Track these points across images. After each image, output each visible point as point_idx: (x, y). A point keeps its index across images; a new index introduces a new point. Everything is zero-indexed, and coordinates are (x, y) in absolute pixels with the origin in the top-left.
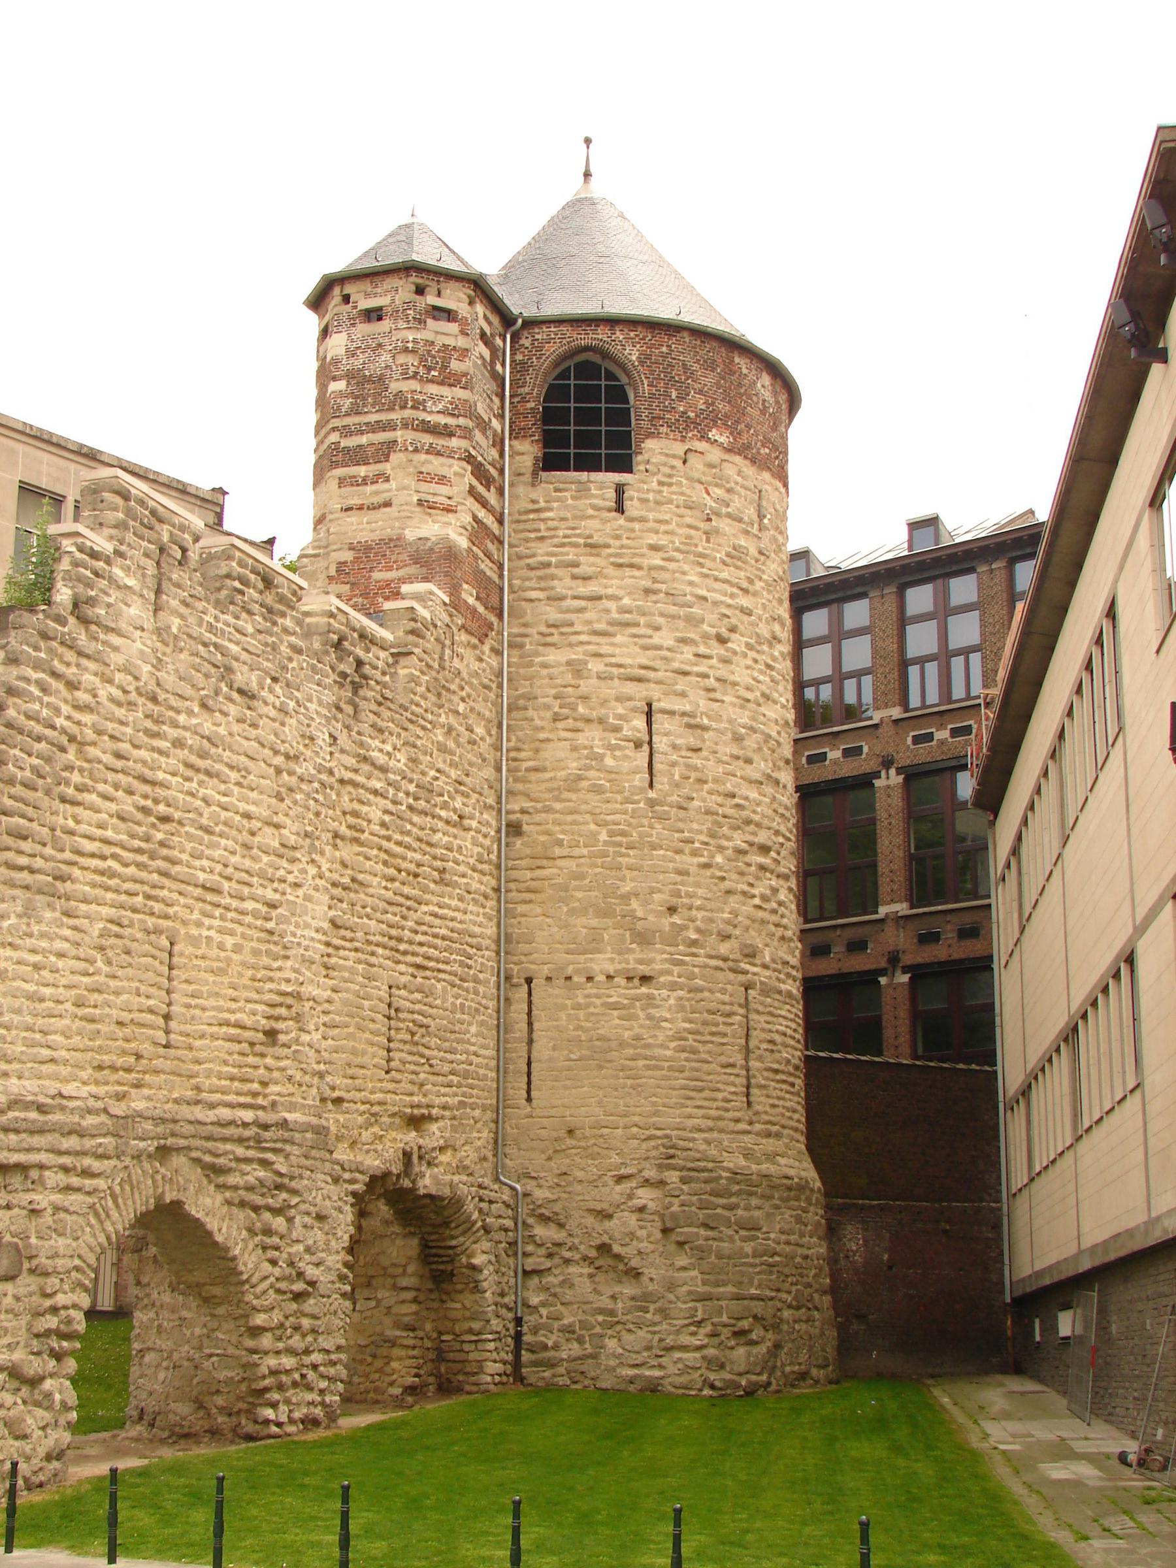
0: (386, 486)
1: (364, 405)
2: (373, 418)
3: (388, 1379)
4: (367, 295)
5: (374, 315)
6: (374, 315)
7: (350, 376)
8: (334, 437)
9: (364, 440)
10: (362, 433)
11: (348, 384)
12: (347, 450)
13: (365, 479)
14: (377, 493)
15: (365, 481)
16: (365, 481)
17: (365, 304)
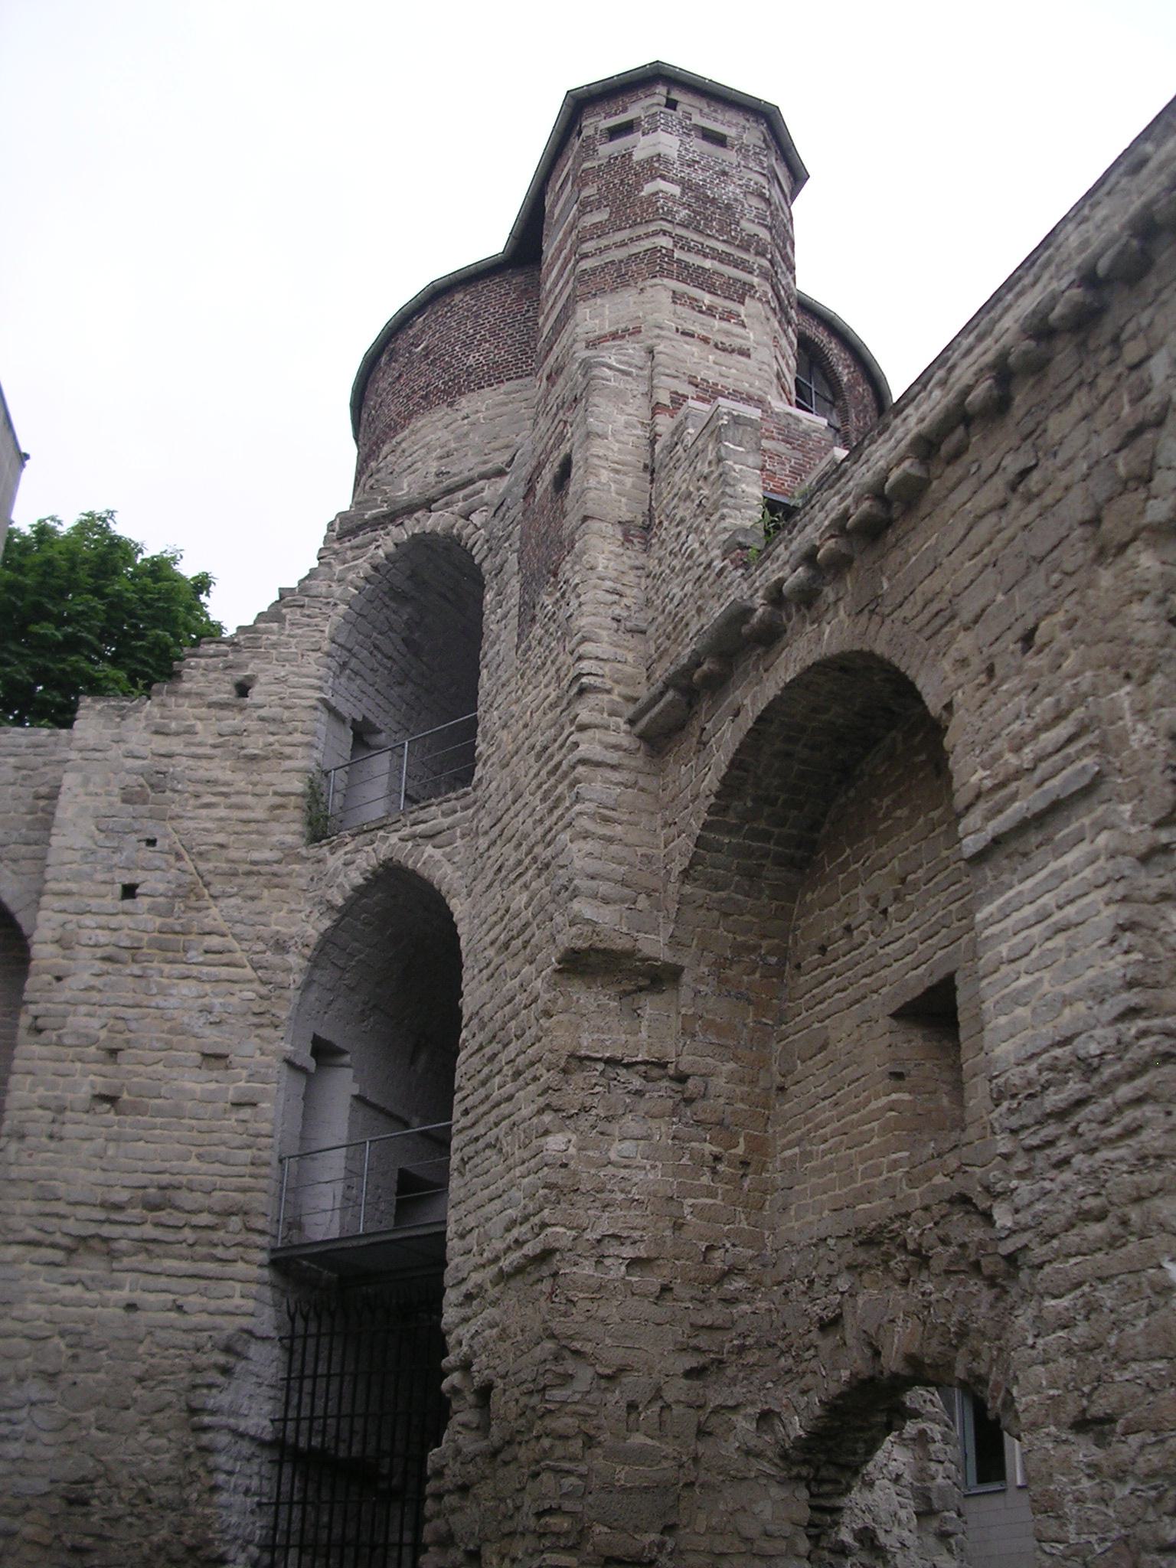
2: (721, 247)
6: (720, 140)
7: (686, 185)
8: (665, 242)
9: (708, 264)
10: (705, 256)
11: (683, 193)
14: (728, 333)
16: (710, 311)
17: (697, 119)
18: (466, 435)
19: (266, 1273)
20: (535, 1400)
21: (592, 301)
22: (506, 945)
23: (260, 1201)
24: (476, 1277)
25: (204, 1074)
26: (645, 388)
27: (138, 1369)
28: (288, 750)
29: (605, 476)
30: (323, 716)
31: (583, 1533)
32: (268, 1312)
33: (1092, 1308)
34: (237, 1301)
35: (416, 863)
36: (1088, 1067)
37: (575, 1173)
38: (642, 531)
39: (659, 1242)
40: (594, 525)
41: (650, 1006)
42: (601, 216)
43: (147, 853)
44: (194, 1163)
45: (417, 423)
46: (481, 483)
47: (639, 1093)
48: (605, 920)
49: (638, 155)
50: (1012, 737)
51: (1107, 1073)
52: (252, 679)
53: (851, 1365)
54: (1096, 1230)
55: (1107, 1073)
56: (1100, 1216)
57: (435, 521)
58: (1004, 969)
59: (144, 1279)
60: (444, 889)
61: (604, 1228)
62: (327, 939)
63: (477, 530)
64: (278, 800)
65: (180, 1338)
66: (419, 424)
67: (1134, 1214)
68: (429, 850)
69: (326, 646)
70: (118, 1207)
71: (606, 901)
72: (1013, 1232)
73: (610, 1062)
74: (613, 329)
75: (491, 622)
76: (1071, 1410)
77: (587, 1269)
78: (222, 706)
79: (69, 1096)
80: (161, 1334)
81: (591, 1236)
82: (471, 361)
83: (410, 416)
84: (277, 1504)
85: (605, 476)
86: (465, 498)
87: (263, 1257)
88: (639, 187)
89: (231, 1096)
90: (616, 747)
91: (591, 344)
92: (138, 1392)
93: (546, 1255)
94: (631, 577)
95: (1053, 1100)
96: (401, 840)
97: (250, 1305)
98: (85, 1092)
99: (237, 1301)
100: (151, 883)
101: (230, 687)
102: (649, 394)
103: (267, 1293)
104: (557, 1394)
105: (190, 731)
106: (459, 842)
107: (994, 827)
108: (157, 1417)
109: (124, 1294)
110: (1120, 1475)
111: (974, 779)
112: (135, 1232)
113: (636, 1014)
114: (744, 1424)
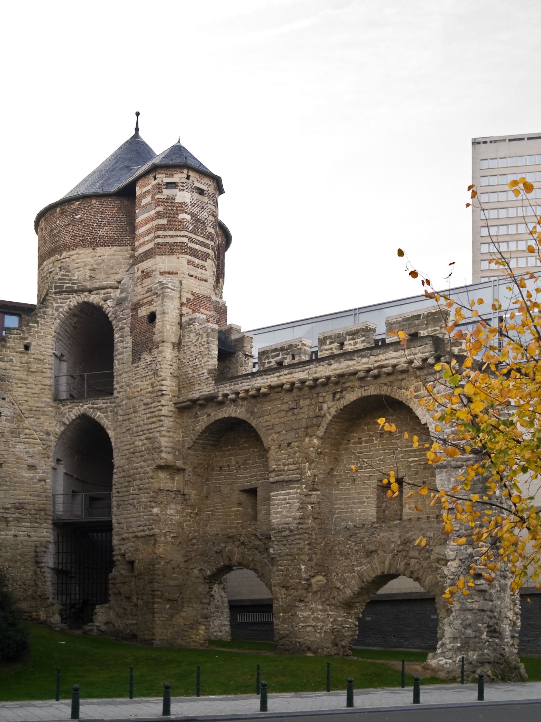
18: (100, 264)
19: (51, 526)
21: (161, 256)
22: (133, 453)
23: (50, 507)
26: (178, 295)
29: (168, 327)
32: (52, 536)
34: (45, 534)
35: (95, 416)
36: (291, 531)
37: (160, 517)
38: (178, 345)
40: (165, 344)
45: (79, 251)
46: (110, 290)
47: (174, 498)
48: (167, 457)
50: (283, 463)
51: (295, 533)
54: (290, 558)
56: (291, 555)
57: (94, 298)
58: (276, 506)
59: (17, 528)
60: (105, 427)
61: (167, 530)
62: (63, 433)
63: (109, 307)
65: (30, 544)
66: (81, 252)
68: (99, 413)
71: (169, 453)
72: (273, 554)
73: (168, 490)
74: (169, 270)
75: (119, 346)
77: (163, 538)
80: (25, 543)
81: (164, 531)
82: (100, 233)
83: (76, 246)
85: (168, 327)
86: (104, 294)
87: (51, 522)
88: (177, 214)
90: (171, 411)
91: (161, 274)
92: (19, 557)
93: (153, 535)
94: (174, 360)
95: (284, 534)
96: (89, 408)
97: (49, 535)
99: (45, 534)
102: (180, 298)
103: (51, 531)
106: (109, 413)
107: (277, 478)
108: (26, 564)
109: (13, 532)
111: (273, 467)
113: (173, 479)
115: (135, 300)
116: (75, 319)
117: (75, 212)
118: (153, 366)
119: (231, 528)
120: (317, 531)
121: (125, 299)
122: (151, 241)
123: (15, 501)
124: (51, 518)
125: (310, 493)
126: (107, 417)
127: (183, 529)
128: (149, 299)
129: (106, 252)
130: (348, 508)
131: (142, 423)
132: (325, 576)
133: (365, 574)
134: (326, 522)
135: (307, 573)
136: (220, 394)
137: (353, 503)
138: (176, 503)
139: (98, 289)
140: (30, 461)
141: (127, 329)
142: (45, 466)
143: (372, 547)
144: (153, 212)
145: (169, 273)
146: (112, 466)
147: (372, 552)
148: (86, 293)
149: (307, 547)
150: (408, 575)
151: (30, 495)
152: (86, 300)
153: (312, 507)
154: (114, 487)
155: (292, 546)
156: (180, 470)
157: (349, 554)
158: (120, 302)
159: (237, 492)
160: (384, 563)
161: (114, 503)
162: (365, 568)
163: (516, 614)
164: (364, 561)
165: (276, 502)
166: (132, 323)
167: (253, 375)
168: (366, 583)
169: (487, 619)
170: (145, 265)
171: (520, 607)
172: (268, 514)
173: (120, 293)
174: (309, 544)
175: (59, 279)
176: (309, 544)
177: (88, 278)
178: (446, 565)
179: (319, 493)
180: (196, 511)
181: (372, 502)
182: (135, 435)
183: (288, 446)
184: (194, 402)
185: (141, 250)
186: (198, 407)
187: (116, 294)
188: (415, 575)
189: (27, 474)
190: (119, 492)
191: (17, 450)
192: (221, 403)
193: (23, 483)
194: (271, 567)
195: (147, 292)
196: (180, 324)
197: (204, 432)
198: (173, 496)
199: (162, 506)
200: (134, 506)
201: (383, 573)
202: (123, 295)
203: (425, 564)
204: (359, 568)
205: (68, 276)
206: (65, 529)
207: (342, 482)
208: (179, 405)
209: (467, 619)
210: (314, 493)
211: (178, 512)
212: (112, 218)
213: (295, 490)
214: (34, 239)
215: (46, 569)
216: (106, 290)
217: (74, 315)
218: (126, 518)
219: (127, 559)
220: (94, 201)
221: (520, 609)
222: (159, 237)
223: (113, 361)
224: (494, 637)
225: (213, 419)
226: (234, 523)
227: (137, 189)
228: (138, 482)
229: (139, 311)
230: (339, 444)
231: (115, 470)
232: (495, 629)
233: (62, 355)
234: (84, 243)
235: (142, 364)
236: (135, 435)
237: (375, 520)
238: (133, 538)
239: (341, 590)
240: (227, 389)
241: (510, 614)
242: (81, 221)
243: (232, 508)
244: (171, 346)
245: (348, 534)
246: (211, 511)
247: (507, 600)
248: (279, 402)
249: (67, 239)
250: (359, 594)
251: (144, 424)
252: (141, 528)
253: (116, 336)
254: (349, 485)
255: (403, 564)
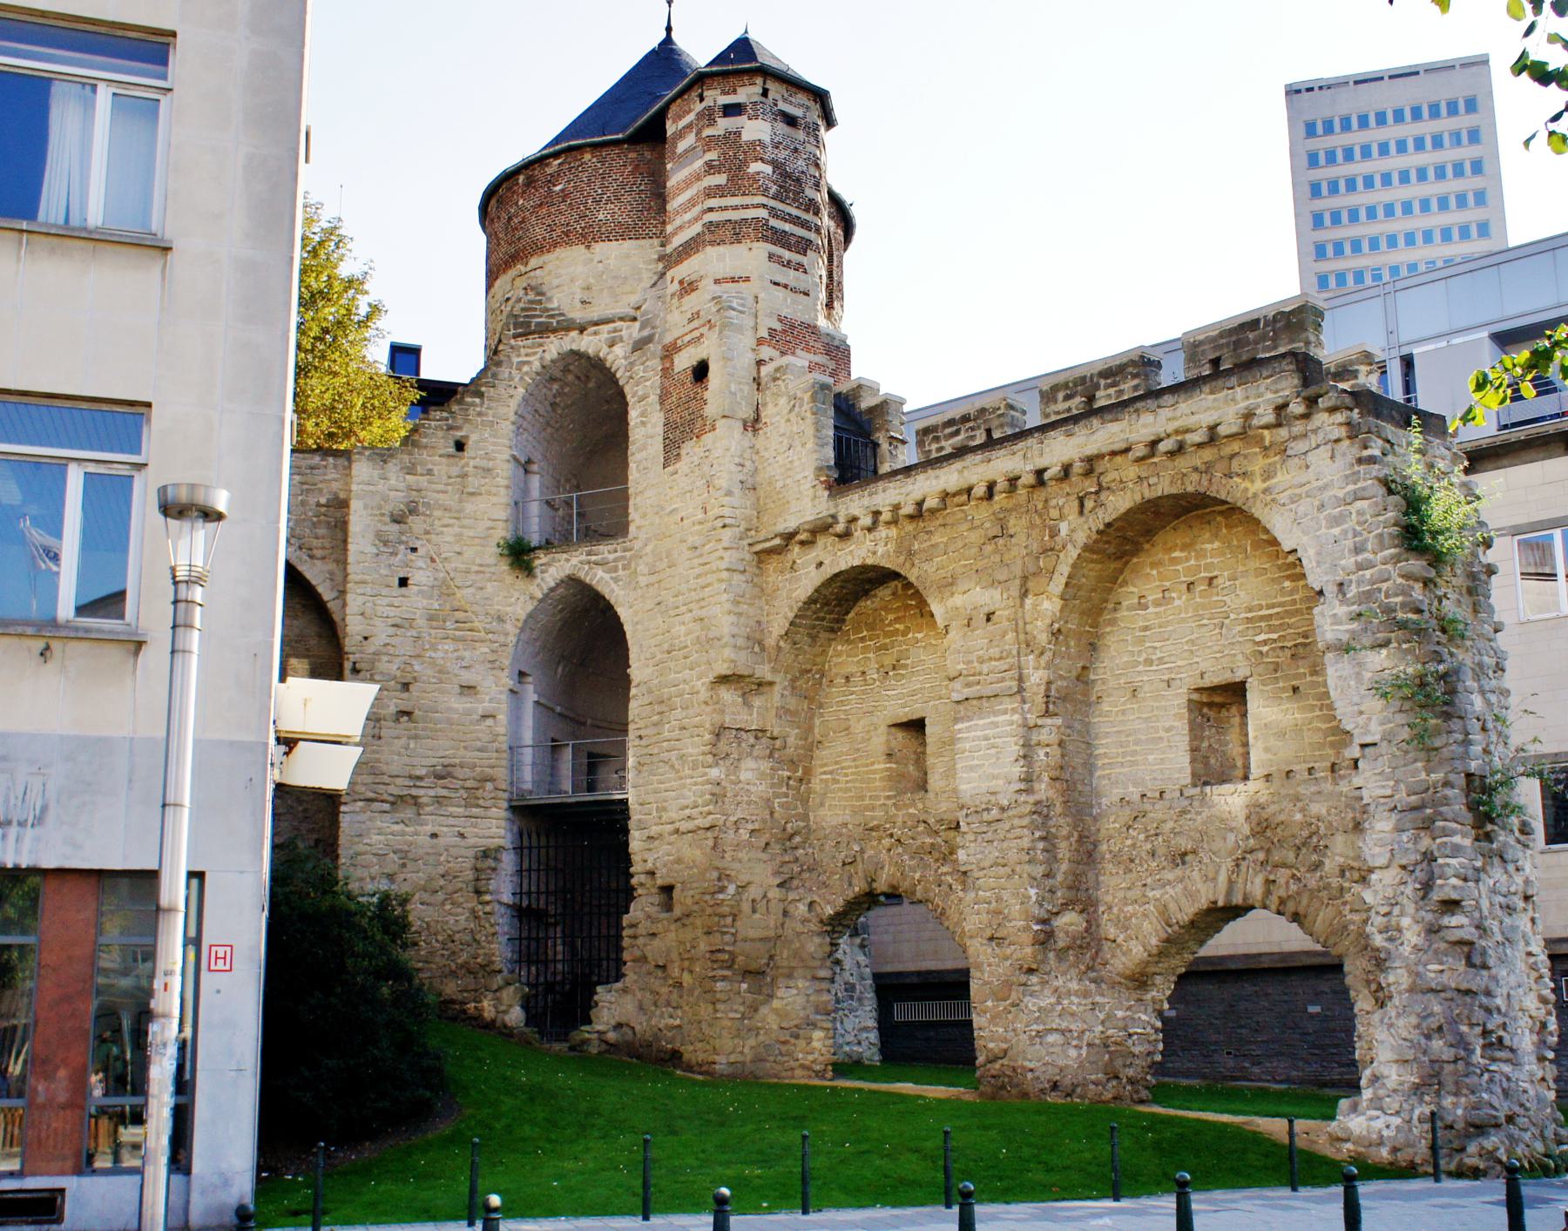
0: (803, 276)
1: (787, 197)
2: (795, 212)
3: (810, 1058)
4: (785, 100)
5: (791, 121)
6: (791, 121)
7: (775, 164)
8: (763, 213)
12: (774, 230)
13: (789, 262)
15: (788, 264)
17: (782, 106)
19: (504, 814)
20: (708, 897)
23: (501, 773)
24: (654, 830)
25: (465, 699)
26: (752, 324)
27: (441, 870)
28: (494, 490)
30: (512, 465)
31: (733, 961)
33: (999, 899)
34: (494, 830)
36: (1003, 809)
39: (764, 821)
41: (757, 702)
42: (721, 179)
43: (413, 556)
44: (462, 752)
45: (561, 253)
49: (746, 136)
52: (467, 437)
53: (858, 887)
55: (1011, 813)
57: (587, 344)
61: (739, 815)
62: (530, 616)
63: (617, 358)
64: (490, 524)
67: (1018, 869)
69: (513, 418)
70: (420, 778)
75: (637, 434)
76: (988, 933)
78: (450, 456)
79: (383, 712)
82: (601, 217)
83: (555, 245)
84: (520, 939)
87: (505, 805)
89: (480, 712)
91: (717, 281)
92: (442, 882)
98: (393, 709)
99: (494, 830)
100: (416, 578)
101: (452, 444)
103: (503, 823)
104: (721, 896)
105: (430, 472)
106: (621, 572)
107: (967, 692)
110: (1006, 959)
112: (432, 793)
114: (802, 908)
115: (668, 339)
116: (556, 387)
117: (553, 180)
118: (706, 468)
119: (873, 809)
120: (1059, 809)
121: (648, 340)
122: (696, 219)
123: (434, 761)
124: (505, 795)
125: (1040, 722)
126: (616, 580)
127: (772, 813)
128: (696, 334)
129: (612, 253)
130: (1124, 754)
131: (684, 587)
132: (1082, 912)
133: (1172, 906)
134: (1080, 787)
135: (1041, 906)
136: (842, 519)
137: (1137, 742)
138: (757, 758)
139: (596, 324)
140: (467, 677)
141: (653, 399)
142: (495, 688)
143: (1185, 844)
144: (699, 164)
145: (733, 280)
146: (626, 682)
147: (1185, 854)
148: (574, 334)
149: (1041, 845)
150: (1274, 907)
151: (465, 748)
152: (574, 347)
153: (1047, 754)
154: (631, 727)
155: (1005, 845)
156: (762, 685)
157: (1132, 861)
158: (639, 345)
159: (883, 729)
160: (1214, 879)
161: (631, 762)
162: (1171, 892)
163: (1543, 1000)
164: (1169, 875)
165: (968, 746)
166: (663, 388)
167: (908, 470)
168: (1176, 928)
169: (1479, 1015)
170: (683, 270)
171: (1552, 985)
172: (951, 772)
173: (641, 329)
174: (1042, 839)
175: (523, 310)
176: (1042, 839)
177: (579, 305)
178: (1363, 880)
179: (1059, 721)
180: (799, 774)
181: (1178, 738)
182: (672, 613)
183: (988, 620)
184: (789, 537)
185: (677, 241)
186: (797, 549)
187: (633, 331)
188: (1290, 907)
189: (459, 704)
190: (640, 737)
191: (440, 654)
192: (845, 536)
193: (450, 722)
194: (961, 894)
195: (690, 321)
196: (757, 381)
197: (811, 601)
198: (752, 740)
199: (728, 762)
200: (672, 766)
201: (1215, 902)
202: (646, 333)
203: (1312, 881)
204: (1157, 894)
205: (540, 302)
206: (534, 818)
207: (1109, 695)
208: (759, 547)
209: (1431, 1015)
210: (1049, 721)
211: (762, 776)
212: (623, 186)
213: (1007, 717)
214: (478, 241)
215: (497, 907)
216: (612, 326)
217: (553, 379)
218: (656, 792)
219: (659, 882)
220: (587, 156)
221: (1553, 990)
222: (711, 210)
223: (626, 465)
224: (1500, 1060)
225: (829, 571)
226: (877, 798)
227: (669, 124)
228: (678, 713)
229: (676, 361)
230: (1100, 611)
231: (633, 691)
232: (1500, 1039)
233: (529, 462)
234: (567, 237)
235: (682, 466)
236: (672, 613)
237: (1189, 780)
238: (671, 834)
239: (1119, 946)
240: (857, 504)
241: (1531, 1003)
242: (565, 195)
243: (873, 764)
244: (740, 425)
245: (1126, 814)
246: (831, 773)
247: (1521, 966)
248: (965, 526)
249: (539, 232)
250: (1162, 954)
251: (690, 590)
252: (687, 812)
253: (633, 415)
254: (1124, 703)
255: (1259, 880)
